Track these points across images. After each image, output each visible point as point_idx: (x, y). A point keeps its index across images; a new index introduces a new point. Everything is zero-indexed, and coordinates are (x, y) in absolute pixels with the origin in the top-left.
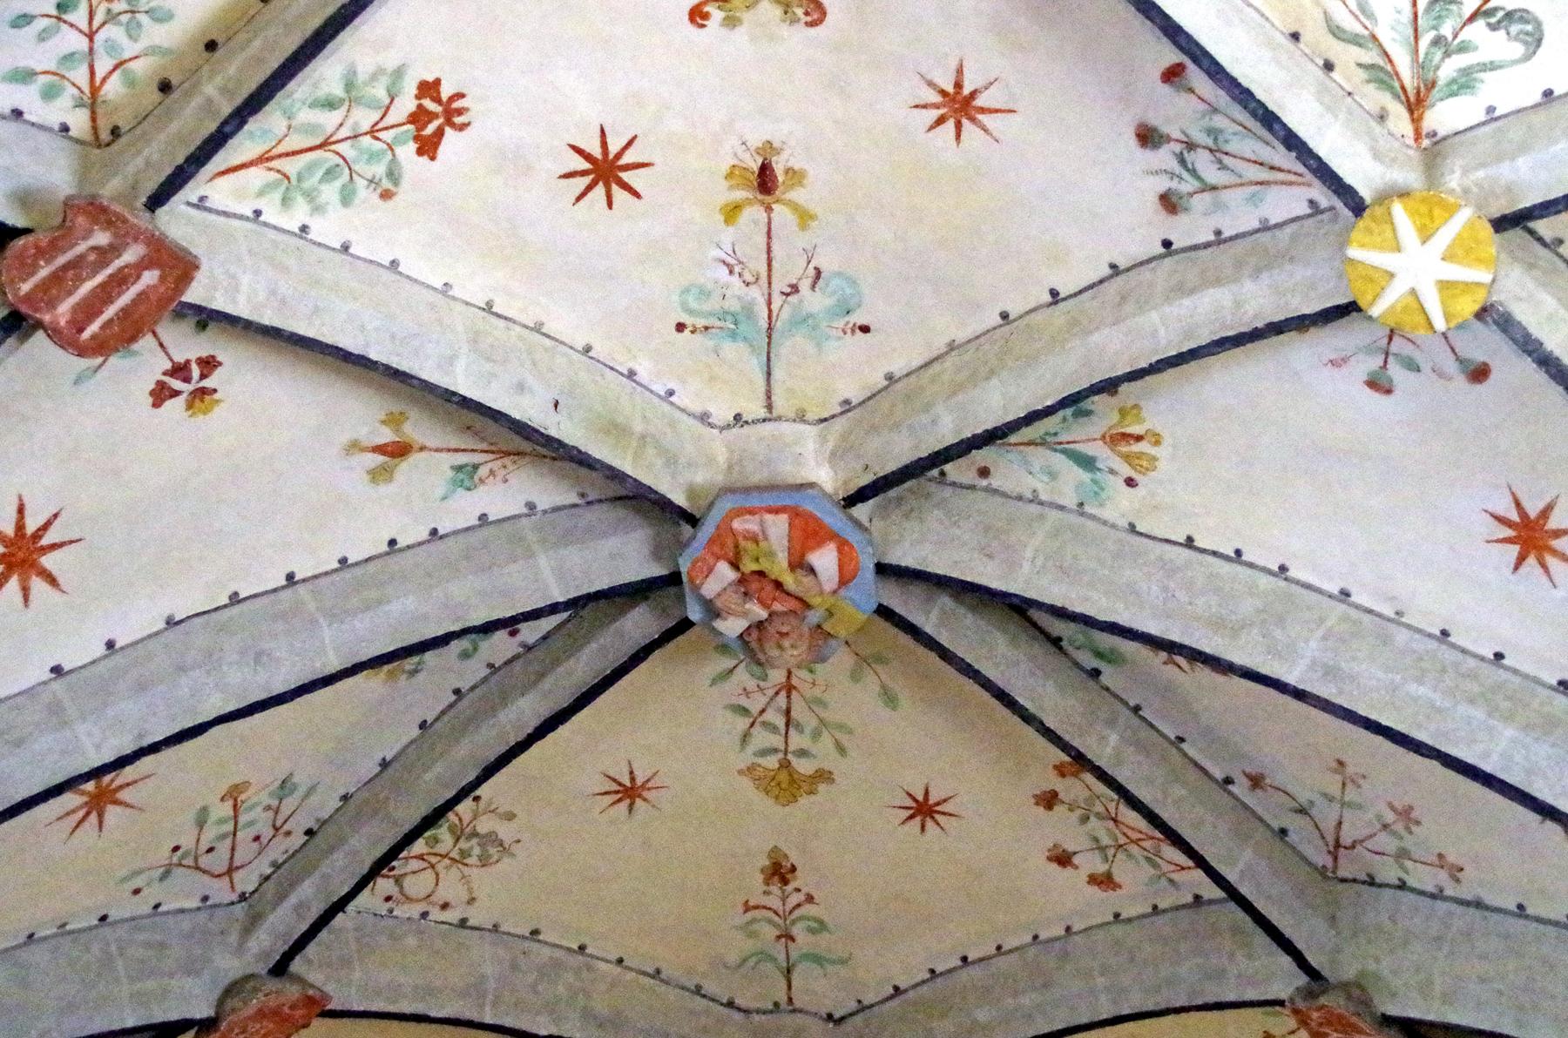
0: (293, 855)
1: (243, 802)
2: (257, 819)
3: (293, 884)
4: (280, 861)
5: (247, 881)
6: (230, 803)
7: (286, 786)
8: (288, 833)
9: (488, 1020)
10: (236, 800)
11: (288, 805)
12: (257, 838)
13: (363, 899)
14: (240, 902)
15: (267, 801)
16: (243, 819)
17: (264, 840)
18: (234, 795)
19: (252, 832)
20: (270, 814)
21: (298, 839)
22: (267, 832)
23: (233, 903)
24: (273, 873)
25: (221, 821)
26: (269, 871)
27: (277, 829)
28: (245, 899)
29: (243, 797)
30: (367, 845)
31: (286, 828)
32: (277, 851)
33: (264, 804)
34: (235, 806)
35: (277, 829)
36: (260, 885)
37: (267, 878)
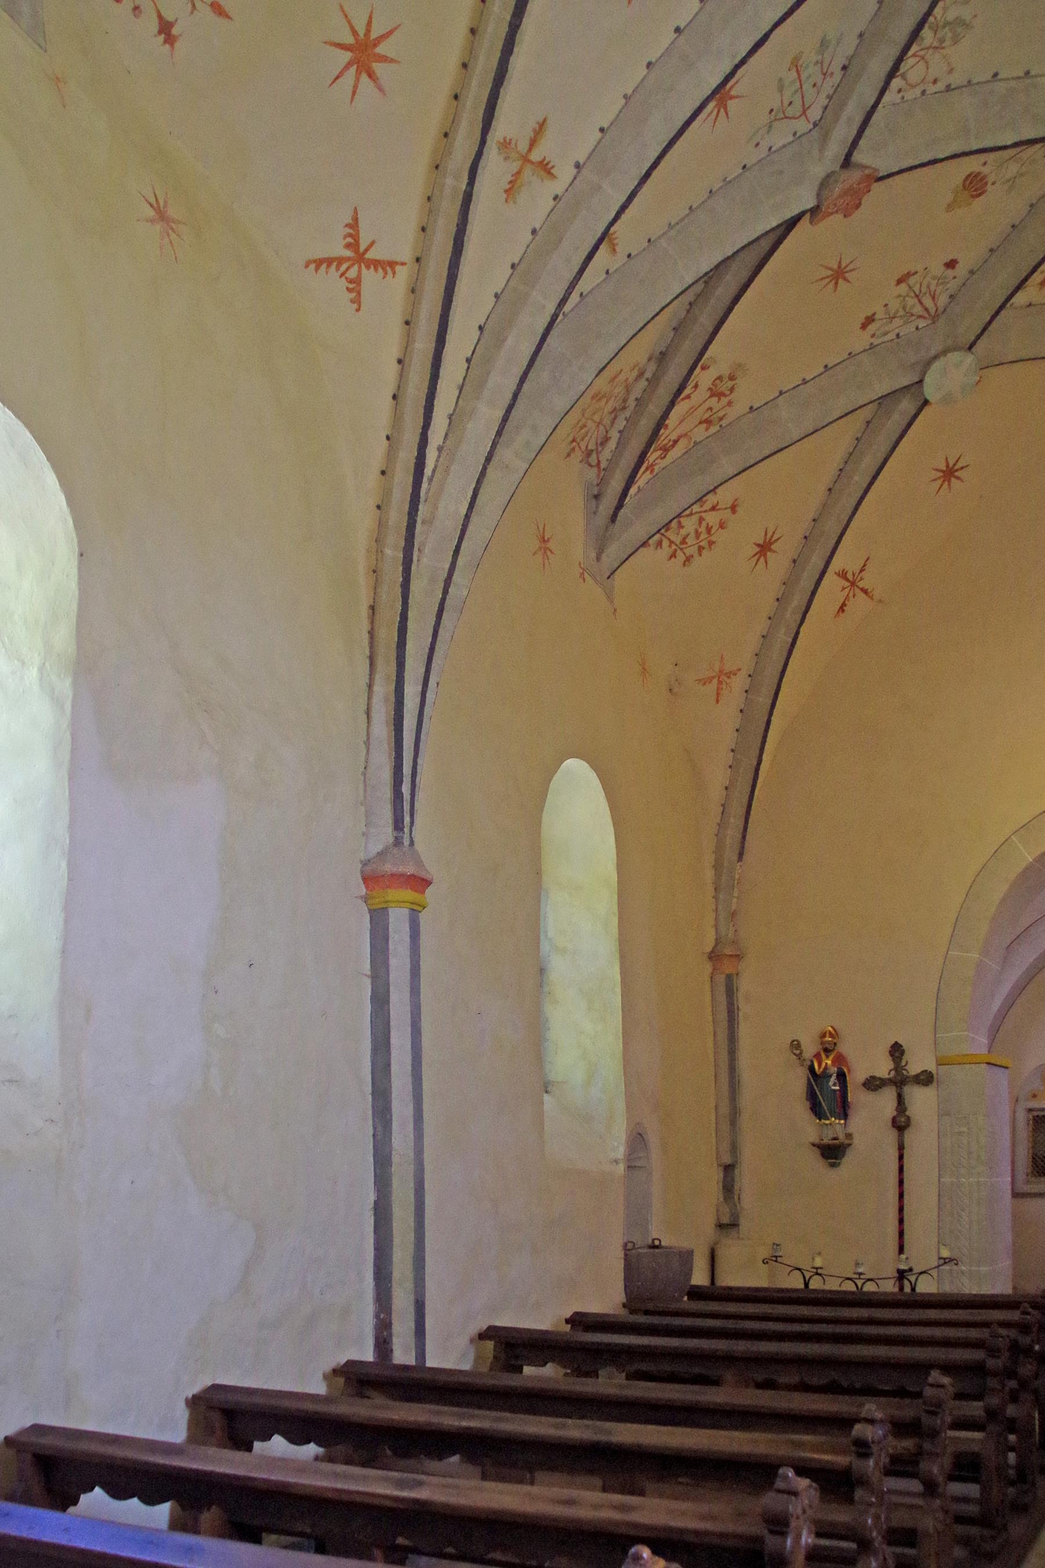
0: (838, 85)
1: (801, 66)
2: (812, 72)
3: (842, 105)
4: (831, 93)
5: (815, 114)
6: (794, 69)
7: (824, 44)
8: (832, 74)
9: (975, 148)
10: (796, 66)
11: (827, 56)
12: (814, 85)
13: (886, 98)
14: (814, 127)
15: (814, 58)
16: (804, 76)
17: (819, 84)
18: (796, 64)
19: (811, 81)
20: (818, 67)
21: (838, 75)
22: (819, 79)
23: (810, 130)
24: (829, 102)
25: (793, 82)
26: (826, 102)
27: (825, 74)
28: (817, 125)
29: (800, 62)
30: (878, 66)
31: (829, 71)
32: (828, 88)
33: (814, 61)
34: (797, 71)
35: (825, 74)
36: (823, 112)
37: (826, 108)
